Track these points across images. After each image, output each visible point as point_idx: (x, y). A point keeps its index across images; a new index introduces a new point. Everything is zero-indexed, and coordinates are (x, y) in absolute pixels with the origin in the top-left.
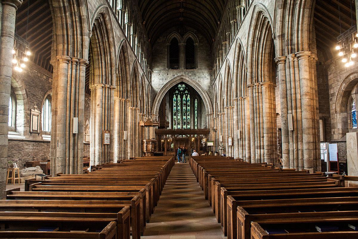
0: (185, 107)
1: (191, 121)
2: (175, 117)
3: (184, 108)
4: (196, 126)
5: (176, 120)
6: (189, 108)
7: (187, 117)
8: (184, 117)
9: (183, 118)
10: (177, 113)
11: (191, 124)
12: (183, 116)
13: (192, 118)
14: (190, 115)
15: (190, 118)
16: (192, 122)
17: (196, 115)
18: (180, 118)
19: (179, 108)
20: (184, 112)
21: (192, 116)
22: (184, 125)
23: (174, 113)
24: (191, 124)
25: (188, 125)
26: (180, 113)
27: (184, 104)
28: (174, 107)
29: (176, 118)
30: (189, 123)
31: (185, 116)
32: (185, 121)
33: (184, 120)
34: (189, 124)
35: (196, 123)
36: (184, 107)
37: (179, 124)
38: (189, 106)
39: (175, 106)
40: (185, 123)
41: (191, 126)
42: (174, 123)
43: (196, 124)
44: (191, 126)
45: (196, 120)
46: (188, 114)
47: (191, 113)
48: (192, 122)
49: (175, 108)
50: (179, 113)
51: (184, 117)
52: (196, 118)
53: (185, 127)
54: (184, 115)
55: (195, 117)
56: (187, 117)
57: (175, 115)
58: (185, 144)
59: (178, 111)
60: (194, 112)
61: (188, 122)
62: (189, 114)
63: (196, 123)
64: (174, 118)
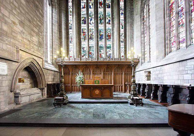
0: (103, 9)
1: (113, 33)
2: (83, 26)
3: (101, 10)
5: (86, 31)
6: (109, 10)
8: (101, 27)
9: (99, 28)
12: (99, 25)
14: (111, 22)
15: (111, 28)
17: (122, 22)
18: (93, 28)
19: (91, 10)
24: (113, 39)
26: (93, 19)
27: (99, 3)
29: (86, 28)
30: (110, 36)
31: (103, 25)
32: (101, 33)
34: (110, 38)
35: (122, 38)
36: (100, 8)
37: (91, 38)
38: (109, 7)
40: (102, 36)
42: (82, 37)
43: (123, 38)
44: (113, 41)
46: (107, 21)
47: (113, 19)
49: (83, 11)
50: (91, 20)
54: (101, 23)
55: (121, 26)
57: (85, 23)
58: (104, 74)
59: (90, 16)
61: (108, 36)
62: (109, 21)
64: (82, 28)
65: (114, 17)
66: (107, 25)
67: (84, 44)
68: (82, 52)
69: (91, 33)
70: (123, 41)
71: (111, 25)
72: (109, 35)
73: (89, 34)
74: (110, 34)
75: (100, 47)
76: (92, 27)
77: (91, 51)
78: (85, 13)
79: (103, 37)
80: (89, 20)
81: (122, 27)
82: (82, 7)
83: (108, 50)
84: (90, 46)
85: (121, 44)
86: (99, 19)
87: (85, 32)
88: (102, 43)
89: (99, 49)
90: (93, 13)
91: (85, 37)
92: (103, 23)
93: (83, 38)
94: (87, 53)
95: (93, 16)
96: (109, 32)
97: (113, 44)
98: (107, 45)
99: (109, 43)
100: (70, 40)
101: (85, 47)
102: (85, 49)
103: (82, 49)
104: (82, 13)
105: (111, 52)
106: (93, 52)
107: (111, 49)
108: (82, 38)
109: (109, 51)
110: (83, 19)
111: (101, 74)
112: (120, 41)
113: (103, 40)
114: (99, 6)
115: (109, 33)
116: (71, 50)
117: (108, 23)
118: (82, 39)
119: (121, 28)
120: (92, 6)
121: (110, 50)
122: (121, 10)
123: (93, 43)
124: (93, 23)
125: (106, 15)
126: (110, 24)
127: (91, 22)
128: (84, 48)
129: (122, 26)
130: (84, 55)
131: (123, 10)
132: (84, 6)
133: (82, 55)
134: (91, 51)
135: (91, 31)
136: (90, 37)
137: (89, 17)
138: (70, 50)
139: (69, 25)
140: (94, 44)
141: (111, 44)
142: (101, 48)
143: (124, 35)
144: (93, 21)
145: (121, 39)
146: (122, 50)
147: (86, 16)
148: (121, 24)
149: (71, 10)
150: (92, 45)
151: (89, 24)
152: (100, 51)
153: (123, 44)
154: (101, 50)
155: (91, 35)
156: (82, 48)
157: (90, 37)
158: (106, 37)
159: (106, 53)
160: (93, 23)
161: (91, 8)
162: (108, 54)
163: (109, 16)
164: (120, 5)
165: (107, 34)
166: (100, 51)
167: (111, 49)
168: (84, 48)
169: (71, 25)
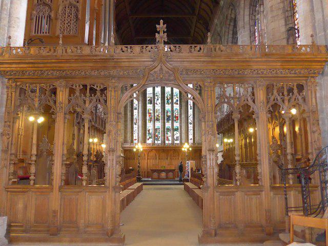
2: (149, 107)
4: (191, 123)
5: (152, 112)
7: (172, 107)
8: (168, 107)
10: (154, 98)
11: (181, 121)
12: (166, 105)
13: (183, 108)
14: (178, 102)
15: (178, 108)
16: (183, 116)
18: (160, 108)
21: (183, 104)
22: (168, 120)
23: (148, 99)
26: (160, 99)
29: (152, 108)
31: (170, 105)
32: (169, 114)
34: (178, 119)
35: (191, 119)
37: (158, 120)
40: (169, 117)
41: (181, 123)
42: (148, 118)
43: (192, 119)
45: (190, 112)
46: (175, 101)
48: (183, 116)
50: (158, 100)
52: (191, 109)
53: (170, 126)
54: (168, 103)
56: (172, 107)
57: (151, 103)
61: (176, 117)
62: (177, 101)
63: (191, 119)
64: (148, 108)
66: (174, 105)
67: (150, 126)
68: (147, 134)
71: (179, 105)
73: (156, 115)
76: (158, 107)
77: (157, 134)
78: (152, 92)
80: (156, 100)
83: (175, 133)
84: (156, 127)
85: (189, 125)
86: (166, 99)
87: (151, 113)
88: (168, 125)
90: (160, 93)
94: (153, 136)
95: (160, 96)
96: (176, 113)
97: (181, 126)
99: (176, 125)
100: (135, 121)
102: (151, 131)
105: (178, 135)
108: (147, 119)
110: (149, 99)
111: (167, 159)
112: (188, 123)
113: (170, 121)
118: (147, 121)
119: (189, 109)
123: (158, 125)
125: (174, 94)
126: (177, 104)
130: (150, 138)
133: (148, 137)
134: (157, 134)
137: (156, 97)
141: (179, 126)
144: (160, 101)
145: (189, 120)
147: (152, 96)
148: (189, 104)
151: (156, 105)
153: (192, 125)
155: (158, 116)
159: (173, 135)
162: (175, 137)
163: (177, 95)
165: (174, 115)
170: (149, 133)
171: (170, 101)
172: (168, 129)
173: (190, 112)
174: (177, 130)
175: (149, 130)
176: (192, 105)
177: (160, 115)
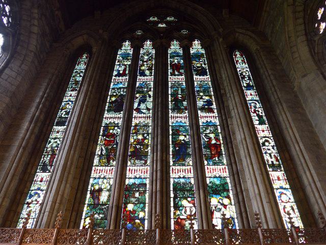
7: (194, 119)
8: (180, 119)
10: (132, 98)
14: (214, 106)
18: (150, 121)
19: (147, 79)
20: (174, 95)
25: (210, 158)
28: (119, 75)
30: (217, 146)
32: (182, 138)
33: (176, 133)
34: (219, 154)
35: (270, 153)
37: (139, 155)
39: (124, 74)
46: (200, 103)
50: (143, 100)
51: (180, 119)
54: (178, 108)
55: (255, 118)
56: (194, 119)
60: (243, 96)
61: (209, 145)
65: (222, 92)
69: (140, 137)
70: (275, 162)
71: (216, 114)
72: (214, 142)
73: (132, 140)
74: (217, 139)
75: (175, 189)
76: (143, 117)
77: (130, 207)
79: (190, 151)
81: (257, 118)
82: (115, 73)
83: (214, 201)
85: (274, 175)
87: (113, 135)
88: (181, 173)
89: (172, 195)
91: (115, 150)
92: (186, 109)
93: (104, 152)
95: (151, 93)
97: (236, 174)
98: (208, 181)
99: (216, 172)
101: (105, 185)
102: (104, 197)
103: (88, 195)
104: (112, 86)
106: (143, 210)
107: (228, 197)
108: (98, 152)
109: (220, 206)
110: (113, 99)
113: (190, 161)
114: (170, 71)
115: (212, 136)
116: (34, 198)
117: (202, 109)
120: (147, 72)
121: (226, 201)
122: (244, 77)
124: (148, 109)
126: (211, 111)
127: (143, 106)
128: (100, 190)
129: (260, 117)
131: (249, 79)
132: (121, 72)
134: (130, 207)
135: (141, 131)
136: (131, 150)
138: (29, 201)
139: (59, 114)
140: (148, 175)
142: (180, 194)
143: (273, 143)
145: (266, 157)
146: (284, 198)
149: (79, 79)
150: (138, 182)
151: (135, 114)
152: (177, 207)
154: (184, 202)
155: (139, 142)
156: (92, 193)
157: (131, 150)
158: (200, 150)
160: (148, 109)
161: (145, 75)
164: (238, 70)
165: (204, 139)
166: (177, 207)
167: (228, 197)
168: (100, 190)
169: (67, 113)
170: (95, 206)
171: (185, 103)
172: (182, 190)
173: (263, 131)
174: (220, 190)
175: (96, 193)
176: (261, 112)
177: (149, 141)
